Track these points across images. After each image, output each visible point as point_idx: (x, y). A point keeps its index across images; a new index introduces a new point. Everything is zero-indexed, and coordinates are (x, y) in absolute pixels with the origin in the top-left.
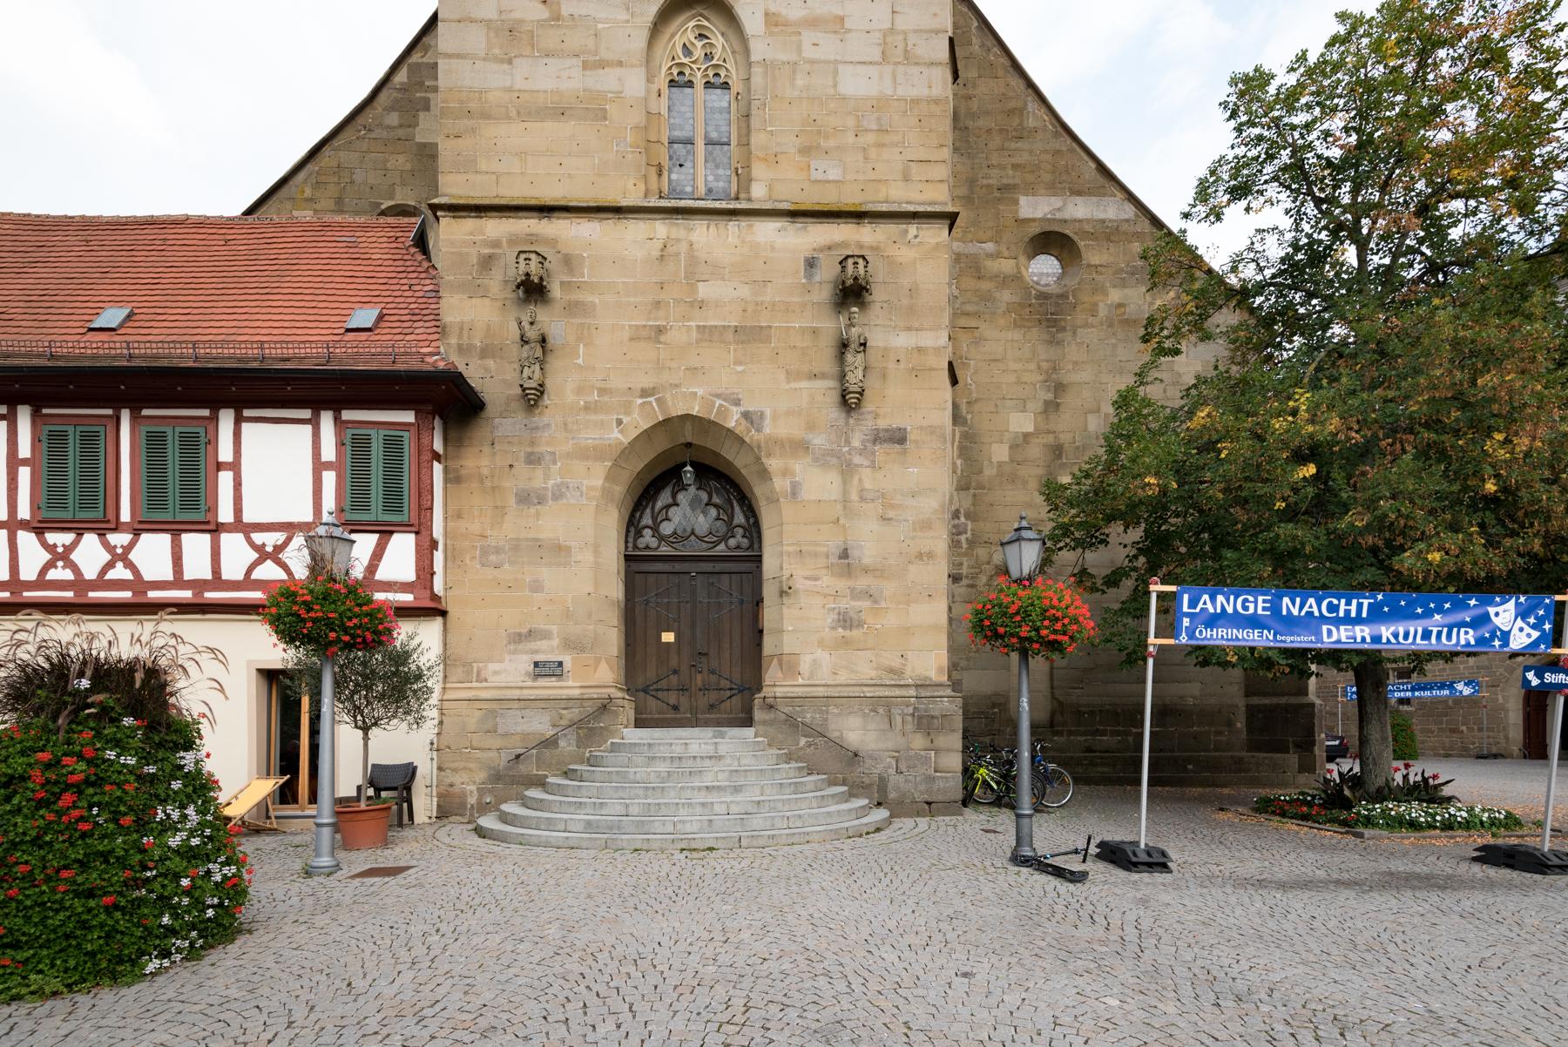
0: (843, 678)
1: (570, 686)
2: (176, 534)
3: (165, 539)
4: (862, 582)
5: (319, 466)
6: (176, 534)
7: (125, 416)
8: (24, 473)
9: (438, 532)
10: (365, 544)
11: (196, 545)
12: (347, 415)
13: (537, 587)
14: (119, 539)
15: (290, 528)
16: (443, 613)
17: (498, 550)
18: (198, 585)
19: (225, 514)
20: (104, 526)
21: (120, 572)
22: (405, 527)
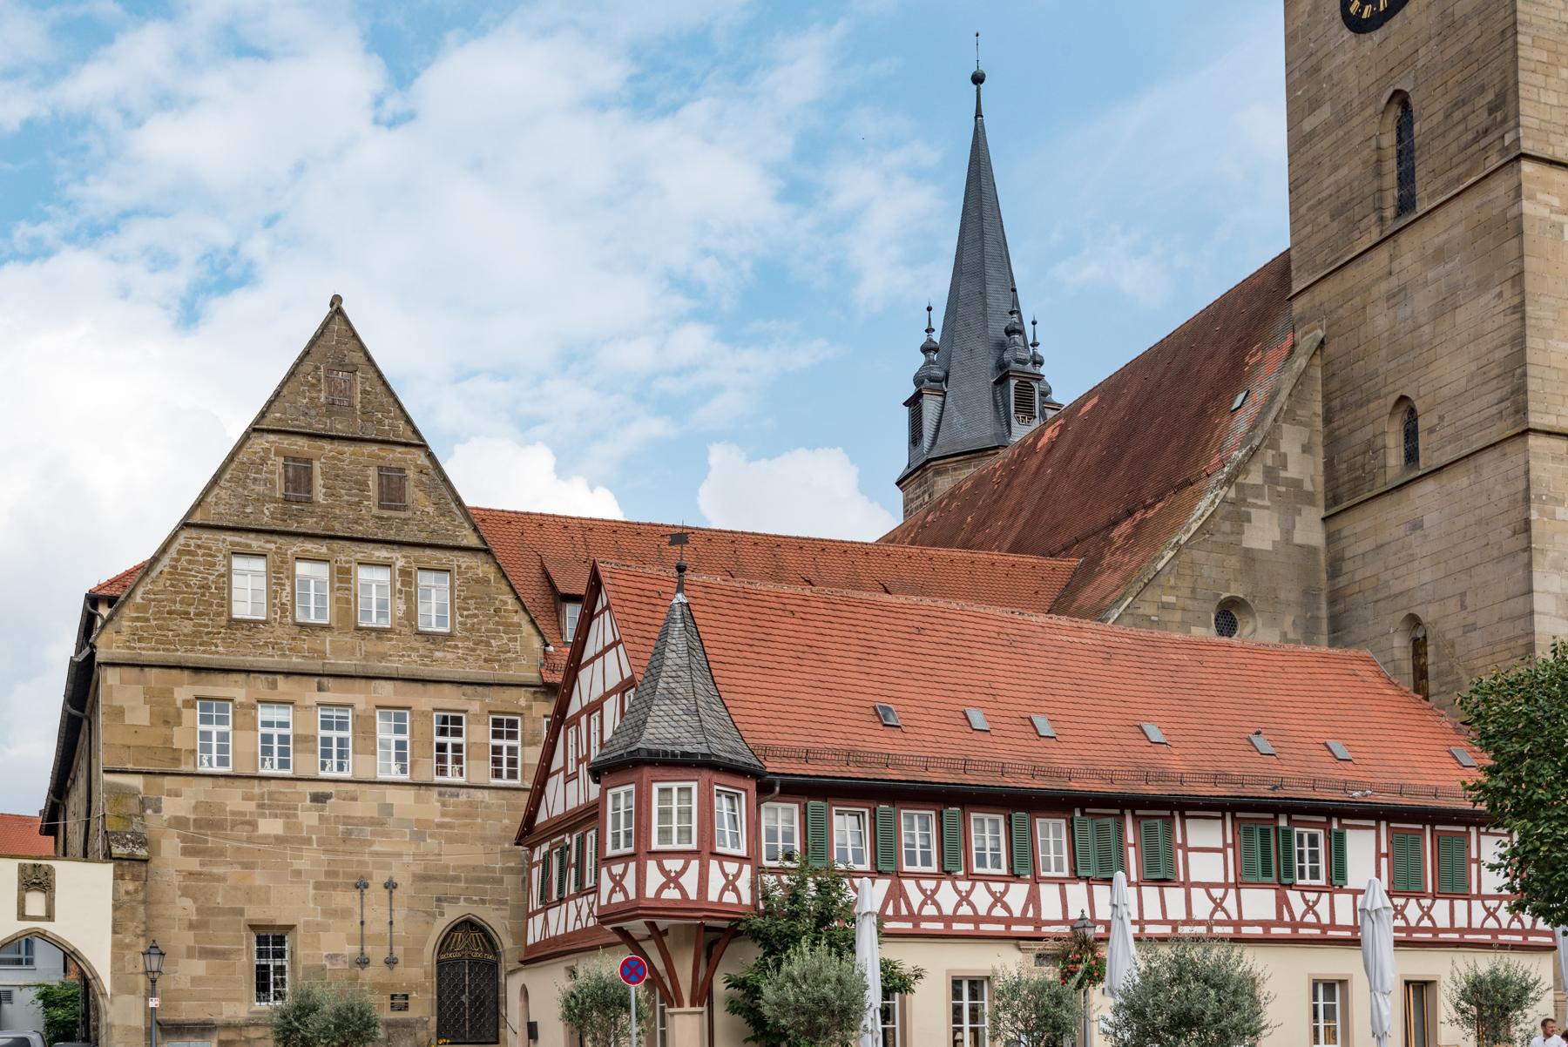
2: (1452, 900)
3: (1447, 902)
6: (1452, 900)
7: (1428, 828)
8: (1384, 861)
11: (1461, 905)
14: (1426, 902)
18: (1461, 931)
19: (1474, 891)
20: (1420, 895)
21: (1426, 923)
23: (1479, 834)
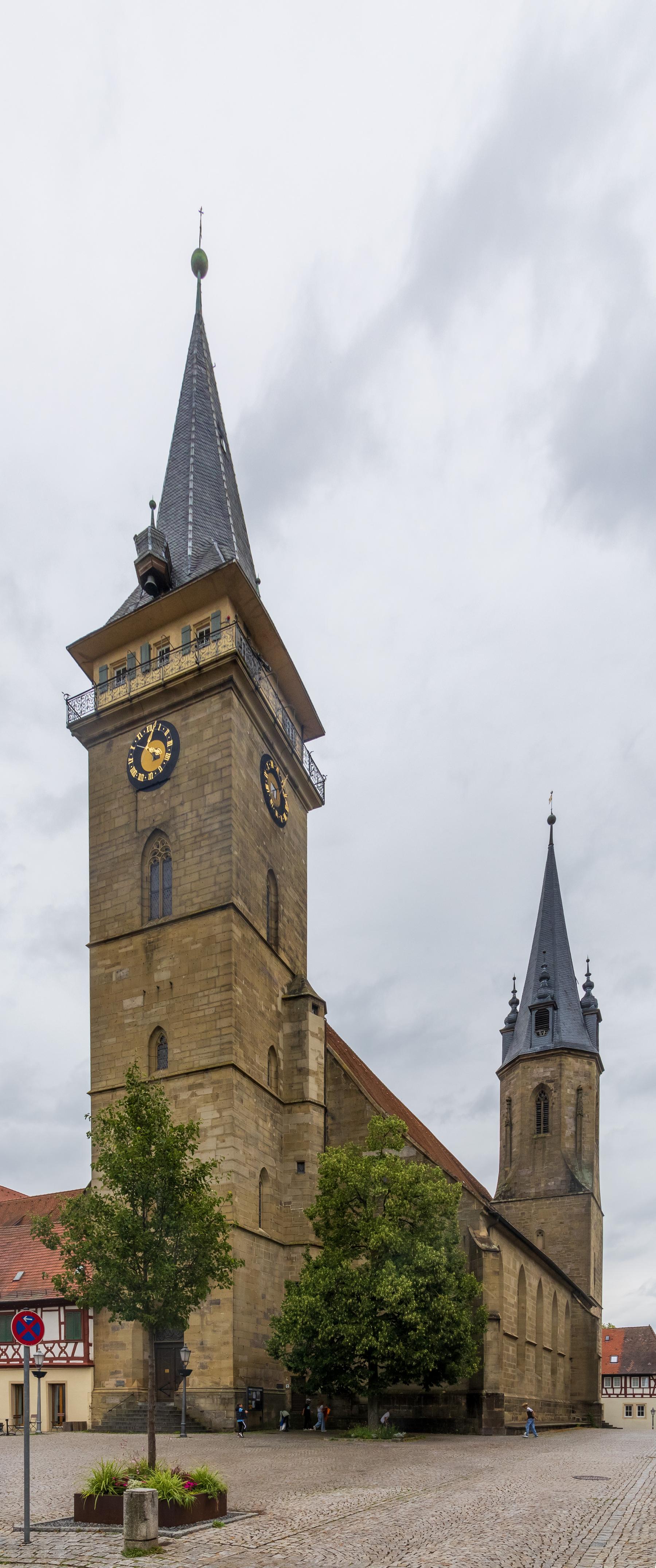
0: (201, 1386)
1: (125, 1389)
4: (207, 1353)
5: (60, 1323)
9: (91, 1340)
10: (71, 1346)
12: (67, 1308)
13: (117, 1357)
15: (54, 1342)
16: (93, 1366)
17: (107, 1346)
22: (80, 1341)
23: (42, 1311)
